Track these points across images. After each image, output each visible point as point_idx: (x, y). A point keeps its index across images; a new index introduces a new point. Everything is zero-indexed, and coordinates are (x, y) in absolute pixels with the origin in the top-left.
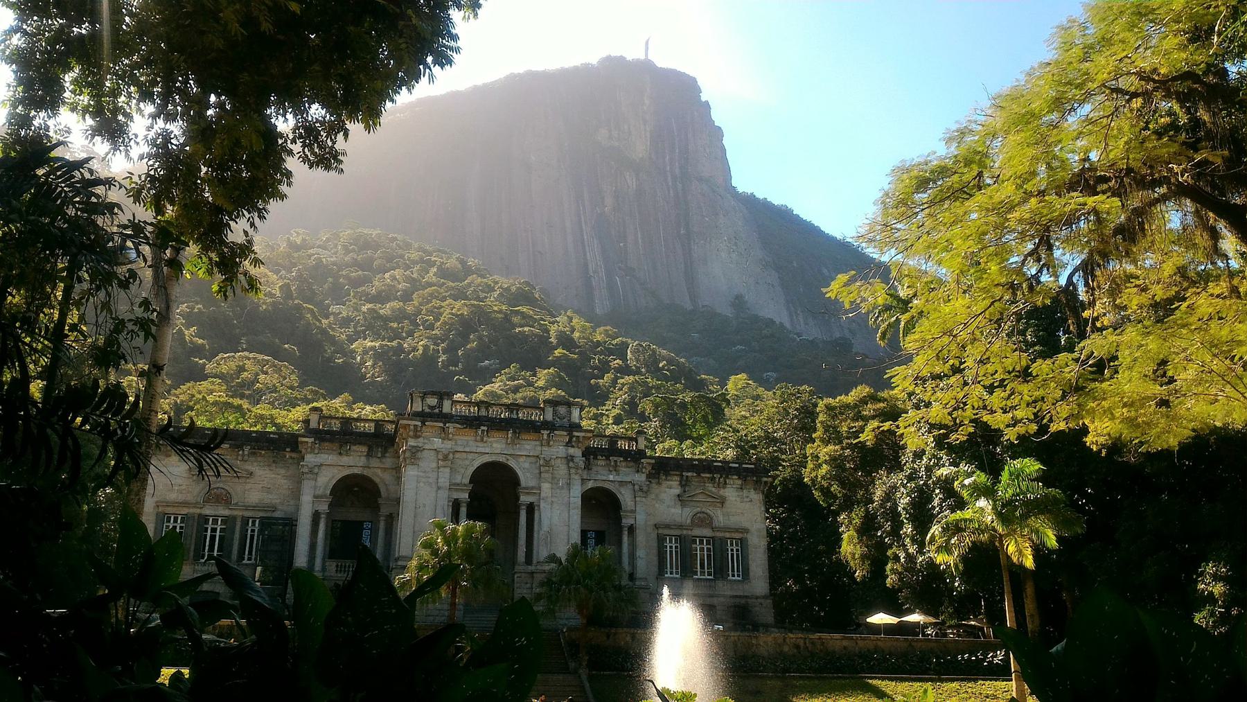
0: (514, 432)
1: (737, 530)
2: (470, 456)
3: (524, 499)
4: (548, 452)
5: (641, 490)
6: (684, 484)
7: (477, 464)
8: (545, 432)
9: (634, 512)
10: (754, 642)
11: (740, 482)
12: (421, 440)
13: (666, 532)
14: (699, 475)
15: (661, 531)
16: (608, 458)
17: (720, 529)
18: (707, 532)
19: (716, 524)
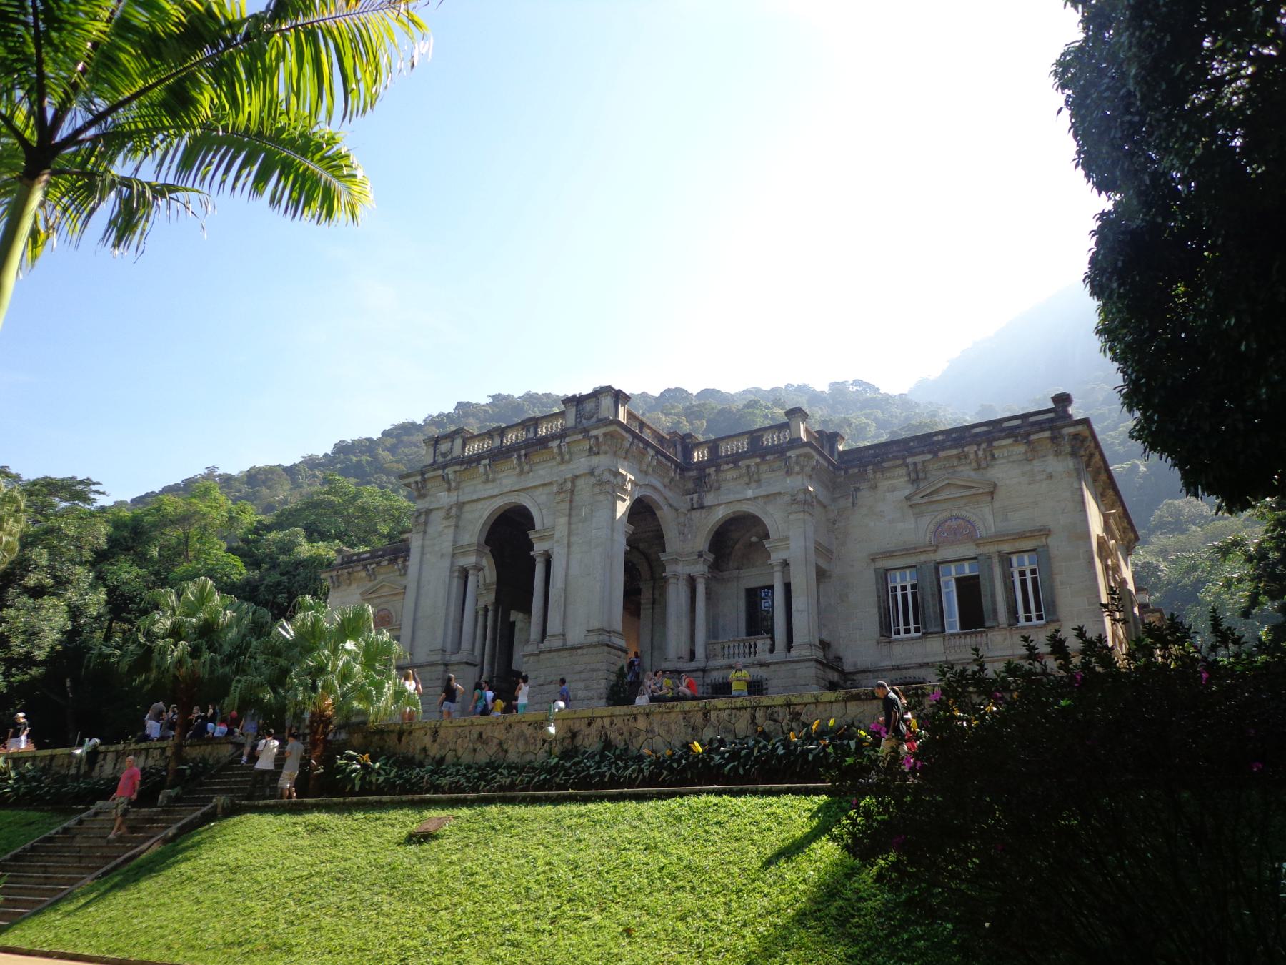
0: (519, 457)
1: (1022, 536)
2: (480, 505)
3: (538, 548)
4: (567, 471)
5: (794, 501)
6: (916, 478)
7: (487, 514)
8: (554, 444)
9: (787, 538)
10: (642, 724)
11: (1021, 448)
12: (428, 499)
13: (889, 564)
14: (935, 454)
15: (879, 564)
16: (736, 466)
17: (985, 541)
18: (967, 550)
19: (981, 531)
